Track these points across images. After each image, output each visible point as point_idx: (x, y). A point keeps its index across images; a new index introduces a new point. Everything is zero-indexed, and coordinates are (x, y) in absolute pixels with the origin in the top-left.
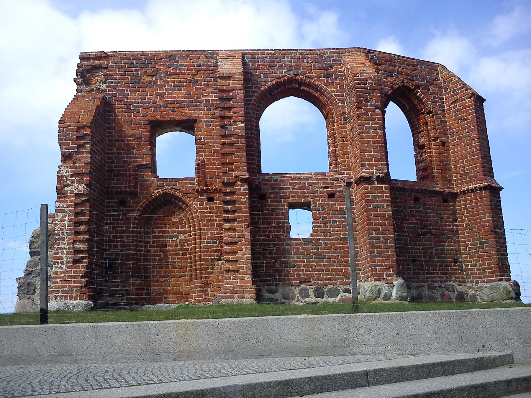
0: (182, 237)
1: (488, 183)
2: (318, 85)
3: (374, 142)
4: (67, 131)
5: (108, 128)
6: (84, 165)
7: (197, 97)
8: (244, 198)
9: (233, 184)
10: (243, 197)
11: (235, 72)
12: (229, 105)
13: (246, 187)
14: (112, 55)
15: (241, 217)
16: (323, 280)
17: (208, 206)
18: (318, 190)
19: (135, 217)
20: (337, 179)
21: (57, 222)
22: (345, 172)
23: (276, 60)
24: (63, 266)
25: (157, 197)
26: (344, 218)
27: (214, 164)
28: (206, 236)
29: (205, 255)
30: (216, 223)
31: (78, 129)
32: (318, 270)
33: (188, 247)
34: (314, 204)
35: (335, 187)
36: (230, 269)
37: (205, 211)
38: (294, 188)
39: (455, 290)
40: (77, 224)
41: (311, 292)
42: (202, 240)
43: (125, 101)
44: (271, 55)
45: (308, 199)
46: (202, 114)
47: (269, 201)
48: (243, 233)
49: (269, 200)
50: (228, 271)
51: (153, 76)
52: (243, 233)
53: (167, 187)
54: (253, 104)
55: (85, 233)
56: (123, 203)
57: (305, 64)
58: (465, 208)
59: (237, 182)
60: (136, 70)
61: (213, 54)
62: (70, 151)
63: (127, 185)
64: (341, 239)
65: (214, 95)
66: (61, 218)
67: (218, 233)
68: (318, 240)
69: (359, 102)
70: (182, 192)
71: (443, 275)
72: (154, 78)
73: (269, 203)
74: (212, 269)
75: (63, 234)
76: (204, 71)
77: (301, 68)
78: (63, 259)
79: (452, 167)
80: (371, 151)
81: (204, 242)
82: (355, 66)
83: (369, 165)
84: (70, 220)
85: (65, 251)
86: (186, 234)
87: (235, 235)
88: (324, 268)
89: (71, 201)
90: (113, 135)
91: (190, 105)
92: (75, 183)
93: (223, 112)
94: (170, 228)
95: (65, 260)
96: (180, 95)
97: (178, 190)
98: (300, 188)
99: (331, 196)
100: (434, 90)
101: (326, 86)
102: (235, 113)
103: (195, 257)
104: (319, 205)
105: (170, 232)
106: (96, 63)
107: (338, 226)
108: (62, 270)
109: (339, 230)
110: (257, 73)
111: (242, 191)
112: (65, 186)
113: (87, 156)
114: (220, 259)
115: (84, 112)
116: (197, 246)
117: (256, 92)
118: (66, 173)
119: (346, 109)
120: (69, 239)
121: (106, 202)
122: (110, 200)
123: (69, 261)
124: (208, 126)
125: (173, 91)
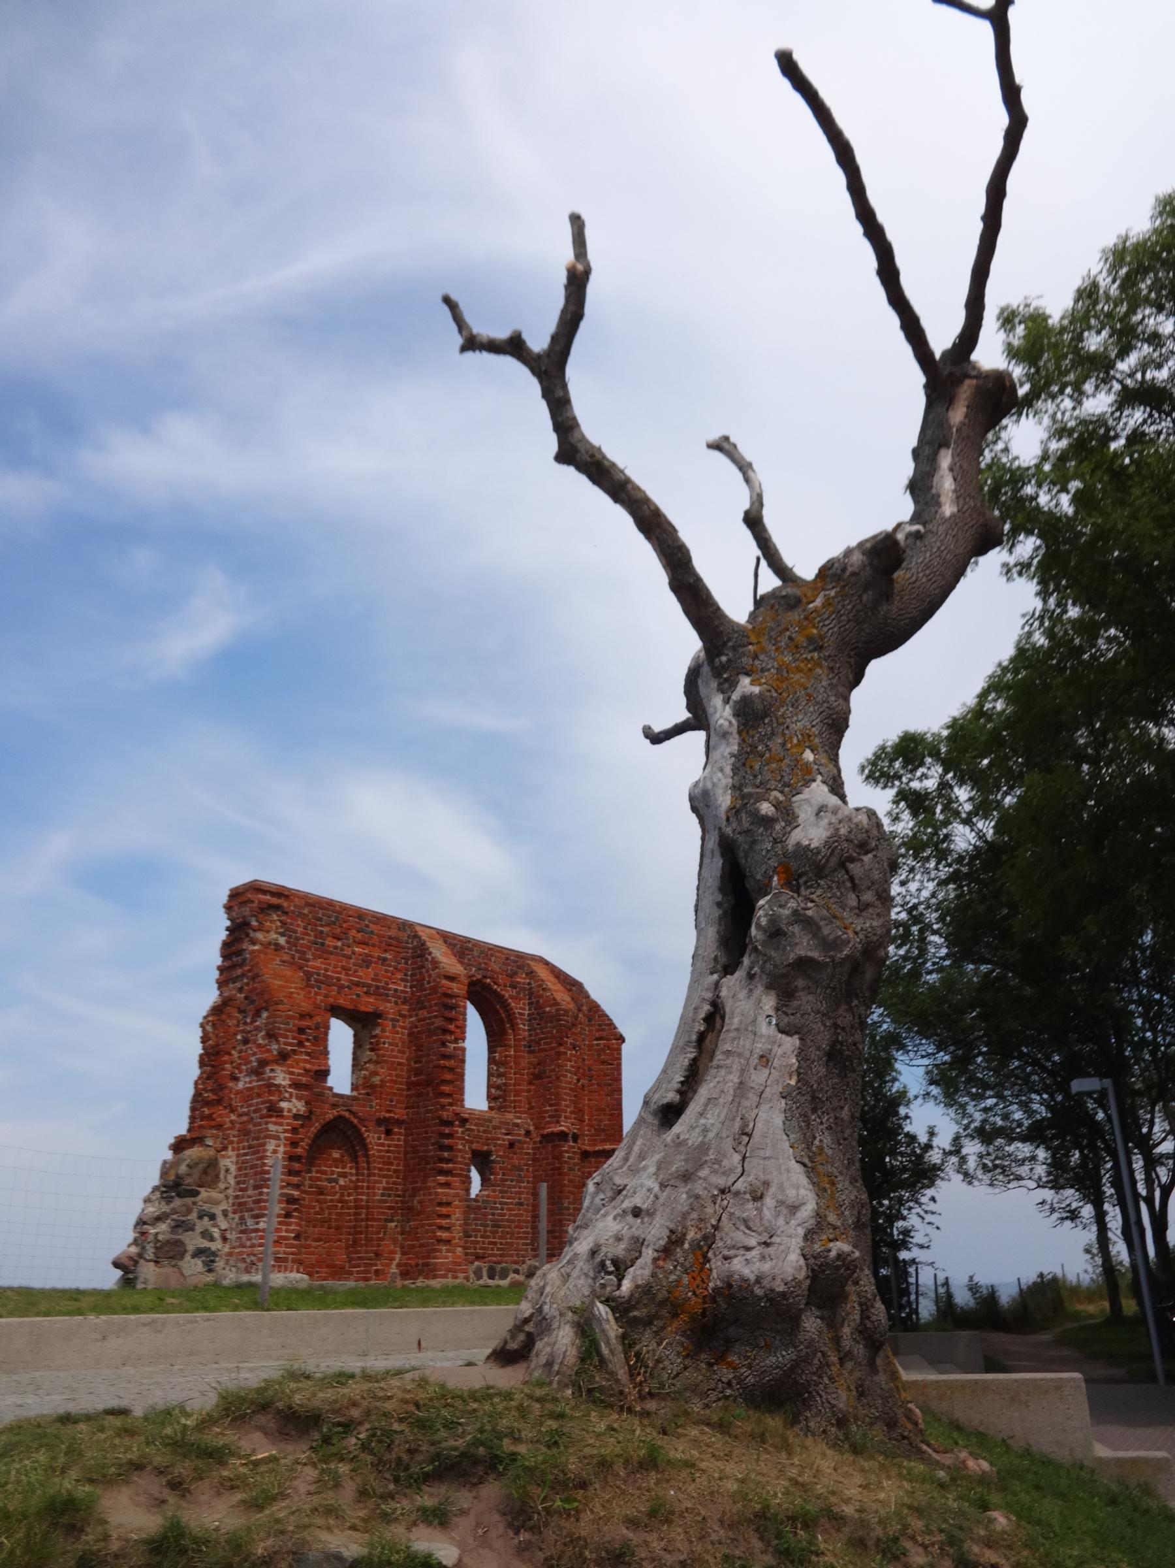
0: (342, 1182)
2: (504, 996)
3: (571, 1089)
4: (289, 1017)
12: (450, 1016)
14: (299, 897)
15: (455, 1169)
16: (495, 1255)
20: (517, 1125)
21: (268, 1154)
25: (331, 1121)
26: (520, 1176)
27: (395, 1082)
38: (479, 1131)
41: (485, 1274)
46: (389, 1008)
50: (440, 1241)
51: (339, 939)
60: (322, 926)
62: (289, 1048)
66: (273, 1147)
68: (495, 1204)
72: (339, 944)
74: (385, 1233)
83: (566, 1117)
84: (285, 1153)
89: (288, 1124)
94: (330, 1166)
96: (366, 975)
98: (485, 1132)
99: (512, 1145)
102: (457, 1027)
104: (501, 1157)
106: (275, 901)
112: (281, 1100)
114: (392, 1221)
115: (295, 988)
124: (394, 1026)
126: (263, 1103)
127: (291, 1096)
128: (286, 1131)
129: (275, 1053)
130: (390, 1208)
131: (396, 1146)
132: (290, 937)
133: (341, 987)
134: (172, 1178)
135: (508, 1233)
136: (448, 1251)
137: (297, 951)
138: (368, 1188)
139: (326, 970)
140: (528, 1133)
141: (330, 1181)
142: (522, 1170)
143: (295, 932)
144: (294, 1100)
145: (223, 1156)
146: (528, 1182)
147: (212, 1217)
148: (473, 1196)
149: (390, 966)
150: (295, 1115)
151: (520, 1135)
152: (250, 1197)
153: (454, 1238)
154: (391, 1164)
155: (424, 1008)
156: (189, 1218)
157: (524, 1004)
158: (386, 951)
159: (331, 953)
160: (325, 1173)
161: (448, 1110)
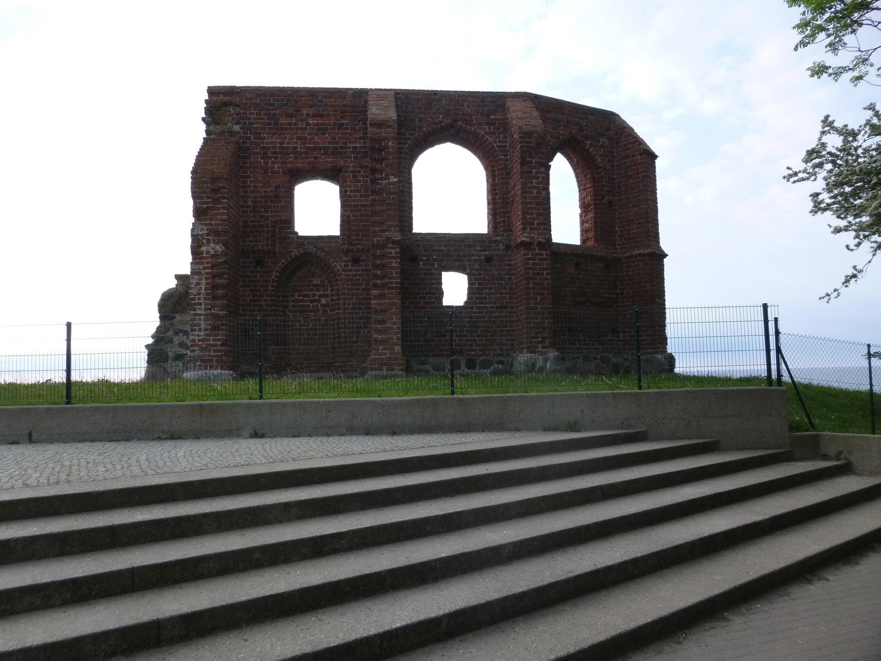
0: (323, 301)
1: (653, 250)
2: (479, 133)
3: (537, 204)
5: (242, 177)
6: (221, 222)
7: (343, 143)
8: (395, 263)
9: (384, 246)
10: (394, 262)
11: (388, 119)
13: (398, 250)
17: (353, 268)
18: (475, 253)
19: (273, 279)
22: (505, 233)
24: (200, 333)
26: (502, 284)
28: (351, 302)
29: (349, 323)
30: (361, 287)
31: (213, 180)
32: (472, 340)
33: (330, 313)
34: (470, 268)
36: (379, 339)
37: (350, 273)
39: (611, 362)
40: (214, 287)
42: (347, 306)
43: (262, 145)
44: (427, 97)
45: (464, 262)
47: (421, 264)
48: (393, 301)
49: (421, 263)
51: (292, 116)
52: (393, 301)
53: (308, 246)
54: (406, 153)
55: (223, 297)
56: (259, 262)
57: (465, 109)
58: (627, 275)
59: (387, 244)
60: (274, 109)
61: (361, 95)
62: (205, 206)
63: (265, 243)
64: (497, 307)
65: (362, 141)
66: (197, 281)
67: (364, 299)
68: (472, 308)
70: (325, 251)
71: (599, 346)
72: (294, 120)
73: (421, 266)
75: (199, 299)
76: (351, 112)
77: (461, 113)
78: (201, 326)
79: (618, 229)
80: (533, 214)
81: (348, 309)
82: (520, 115)
83: (531, 229)
84: (207, 284)
85: (202, 318)
86: (329, 297)
87: (385, 302)
88: (477, 339)
89: (207, 263)
90: (249, 185)
91: (335, 153)
92: (212, 243)
93: (374, 164)
94: (312, 290)
95: (203, 326)
97: (319, 249)
99: (489, 260)
100: (604, 142)
101: (487, 135)
102: (387, 166)
103: (338, 324)
104: (476, 270)
105: (311, 296)
106: (227, 99)
107: (495, 294)
108: (200, 338)
109: (496, 297)
110: (411, 117)
111: (393, 255)
113: (224, 213)
114: (365, 328)
116: (340, 311)
117: (409, 139)
118: (201, 231)
119: (509, 162)
120: (206, 304)
121: (241, 261)
122: (246, 260)
123: (207, 328)
124: (354, 177)
125: (316, 135)
128: (205, 268)
130: (361, 318)
131: (363, 270)
133: (300, 153)
135: (488, 332)
136: (385, 349)
137: (250, 134)
139: (284, 143)
141: (312, 301)
142: (504, 279)
144: (212, 245)
147: (186, 333)
149: (347, 129)
150: (213, 255)
151: (499, 250)
153: (392, 339)
154: (362, 285)
156: (166, 335)
158: (342, 118)
159: (286, 129)
160: (308, 296)
161: (381, 236)
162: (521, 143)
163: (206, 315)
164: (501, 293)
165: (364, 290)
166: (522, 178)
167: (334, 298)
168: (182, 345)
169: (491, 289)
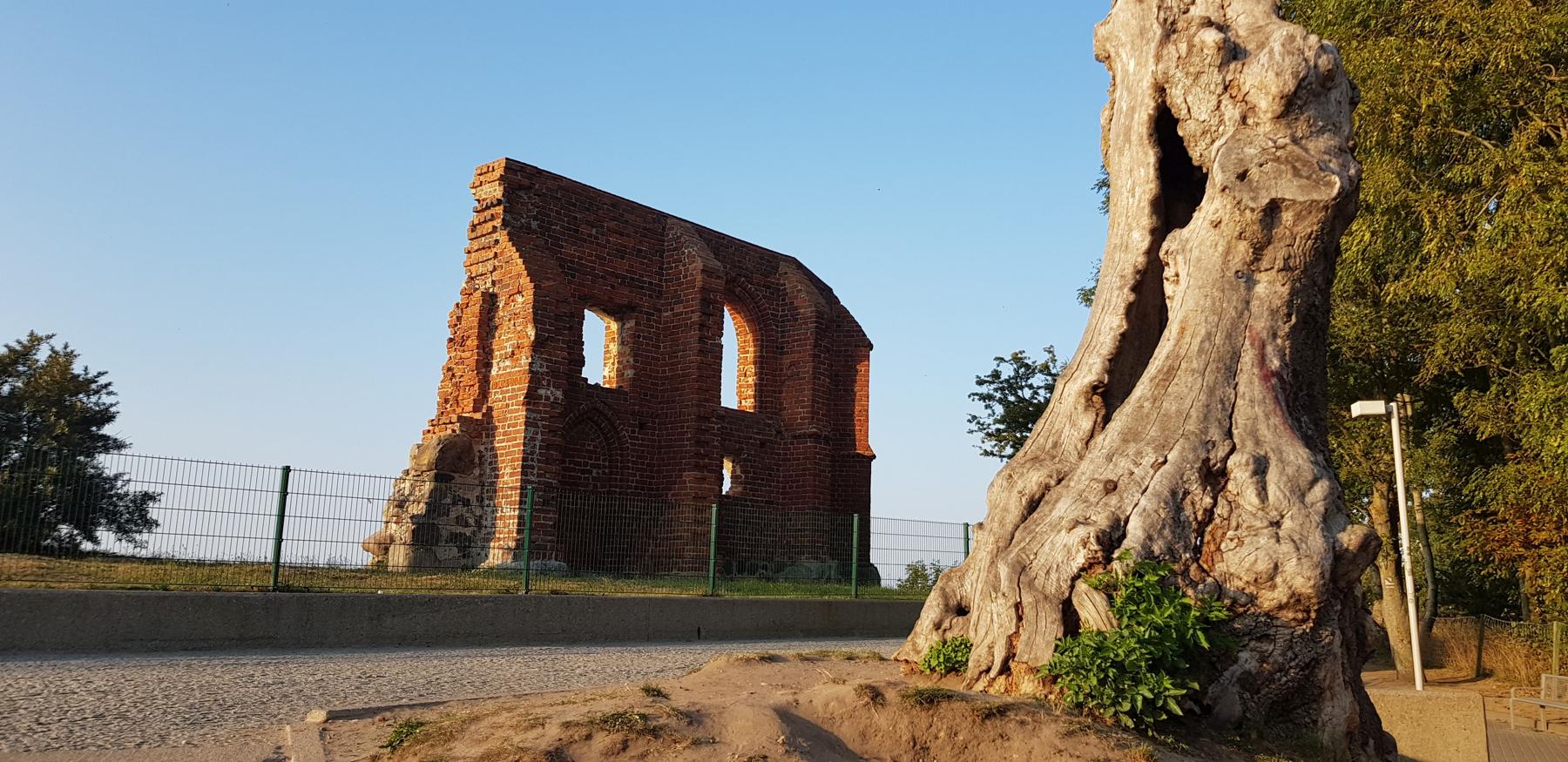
20: (769, 425)
23: (721, 249)
26: (770, 475)
35: (768, 435)
51: (593, 227)
69: (816, 340)
84: (542, 441)
89: (546, 412)
94: (585, 457)
99: (763, 444)
120: (539, 469)
124: (649, 320)
126: (519, 390)
127: (549, 385)
128: (543, 419)
129: (532, 338)
131: (649, 440)
132: (543, 221)
134: (426, 462)
137: (549, 236)
138: (621, 480)
140: (779, 432)
141: (583, 472)
143: (549, 216)
145: (478, 443)
146: (778, 482)
148: (724, 493)
152: (507, 484)
155: (682, 302)
157: (777, 305)
160: (579, 464)
162: (816, 322)
163: (539, 483)
164: (770, 486)
165: (648, 465)
166: (813, 361)
167: (607, 471)
168: (461, 521)
169: (763, 479)
